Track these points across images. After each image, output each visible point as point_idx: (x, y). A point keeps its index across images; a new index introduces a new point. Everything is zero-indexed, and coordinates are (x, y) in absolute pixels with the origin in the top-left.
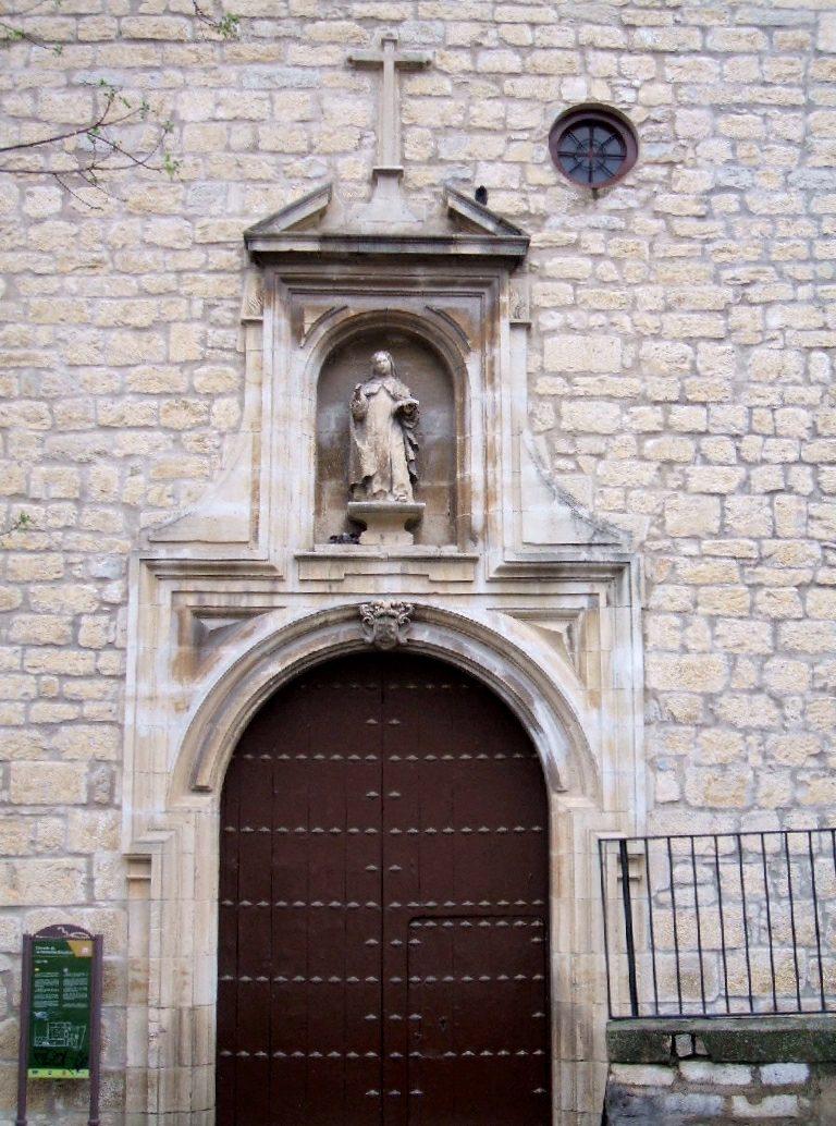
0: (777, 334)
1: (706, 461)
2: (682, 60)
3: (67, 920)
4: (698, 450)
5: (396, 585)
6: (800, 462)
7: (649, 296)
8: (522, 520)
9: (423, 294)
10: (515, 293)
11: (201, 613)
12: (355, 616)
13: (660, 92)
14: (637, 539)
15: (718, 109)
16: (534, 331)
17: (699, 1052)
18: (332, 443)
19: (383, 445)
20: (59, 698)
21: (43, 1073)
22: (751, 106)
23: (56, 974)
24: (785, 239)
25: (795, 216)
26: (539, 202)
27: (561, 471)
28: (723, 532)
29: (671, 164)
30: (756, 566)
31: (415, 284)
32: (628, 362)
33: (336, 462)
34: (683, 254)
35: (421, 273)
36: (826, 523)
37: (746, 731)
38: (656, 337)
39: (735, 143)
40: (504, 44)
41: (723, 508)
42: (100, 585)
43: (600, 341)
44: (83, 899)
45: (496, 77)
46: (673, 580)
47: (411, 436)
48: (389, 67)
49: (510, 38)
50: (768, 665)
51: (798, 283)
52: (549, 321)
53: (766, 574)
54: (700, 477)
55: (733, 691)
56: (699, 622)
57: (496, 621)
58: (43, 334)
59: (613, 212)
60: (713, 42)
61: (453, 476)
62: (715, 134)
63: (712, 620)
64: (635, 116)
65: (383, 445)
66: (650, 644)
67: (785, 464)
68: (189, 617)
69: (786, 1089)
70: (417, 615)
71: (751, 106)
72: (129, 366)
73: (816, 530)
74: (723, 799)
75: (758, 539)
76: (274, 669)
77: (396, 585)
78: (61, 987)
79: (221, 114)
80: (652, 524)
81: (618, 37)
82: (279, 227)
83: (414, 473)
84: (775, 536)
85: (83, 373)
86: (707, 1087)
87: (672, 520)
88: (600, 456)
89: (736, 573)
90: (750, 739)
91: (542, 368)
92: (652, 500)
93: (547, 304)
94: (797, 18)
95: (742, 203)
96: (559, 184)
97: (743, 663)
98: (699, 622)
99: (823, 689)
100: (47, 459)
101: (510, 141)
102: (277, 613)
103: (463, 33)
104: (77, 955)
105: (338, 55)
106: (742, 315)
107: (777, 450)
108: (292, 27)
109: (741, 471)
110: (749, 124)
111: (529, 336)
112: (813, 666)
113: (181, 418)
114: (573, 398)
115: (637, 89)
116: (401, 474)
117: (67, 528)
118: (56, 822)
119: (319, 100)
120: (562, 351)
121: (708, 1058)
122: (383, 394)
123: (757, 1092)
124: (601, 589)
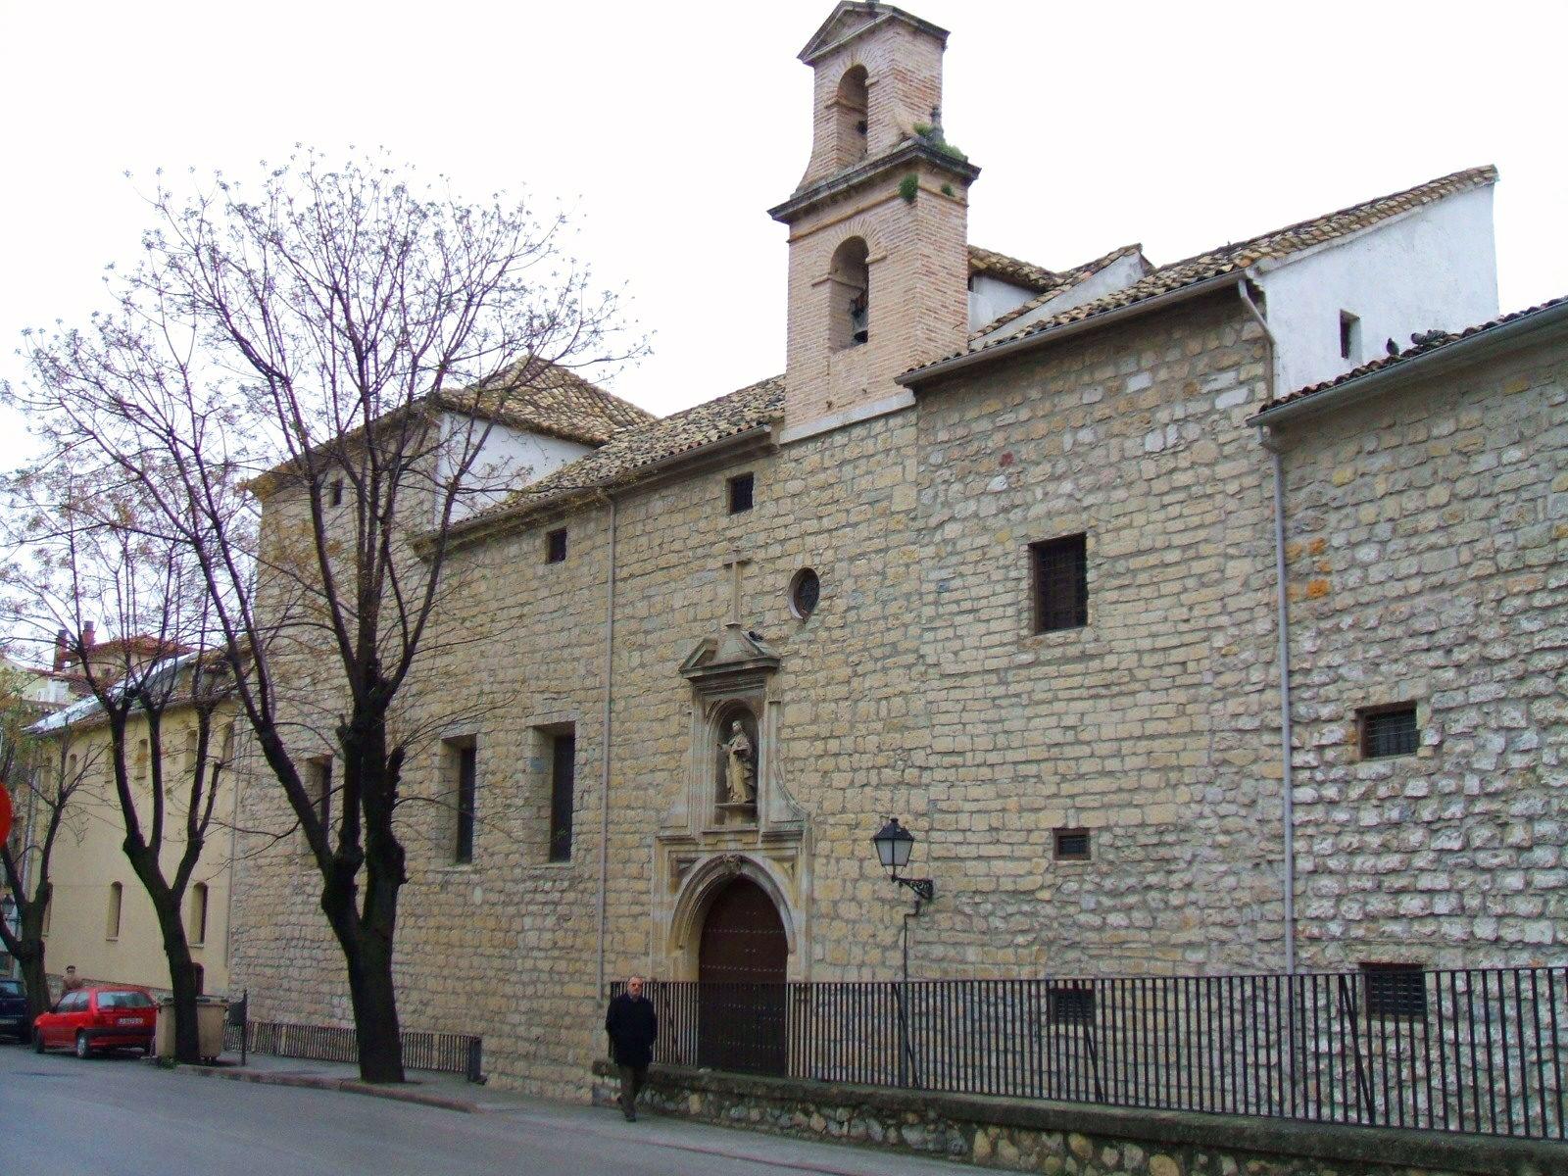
5: (732, 846)
8: (773, 810)
10: (773, 682)
11: (680, 861)
15: (852, 559)
28: (843, 811)
37: (847, 921)
63: (838, 860)
64: (818, 573)
65: (736, 773)
76: (700, 888)
77: (732, 846)
87: (826, 804)
106: (856, 683)
108: (707, 550)
120: (791, 714)
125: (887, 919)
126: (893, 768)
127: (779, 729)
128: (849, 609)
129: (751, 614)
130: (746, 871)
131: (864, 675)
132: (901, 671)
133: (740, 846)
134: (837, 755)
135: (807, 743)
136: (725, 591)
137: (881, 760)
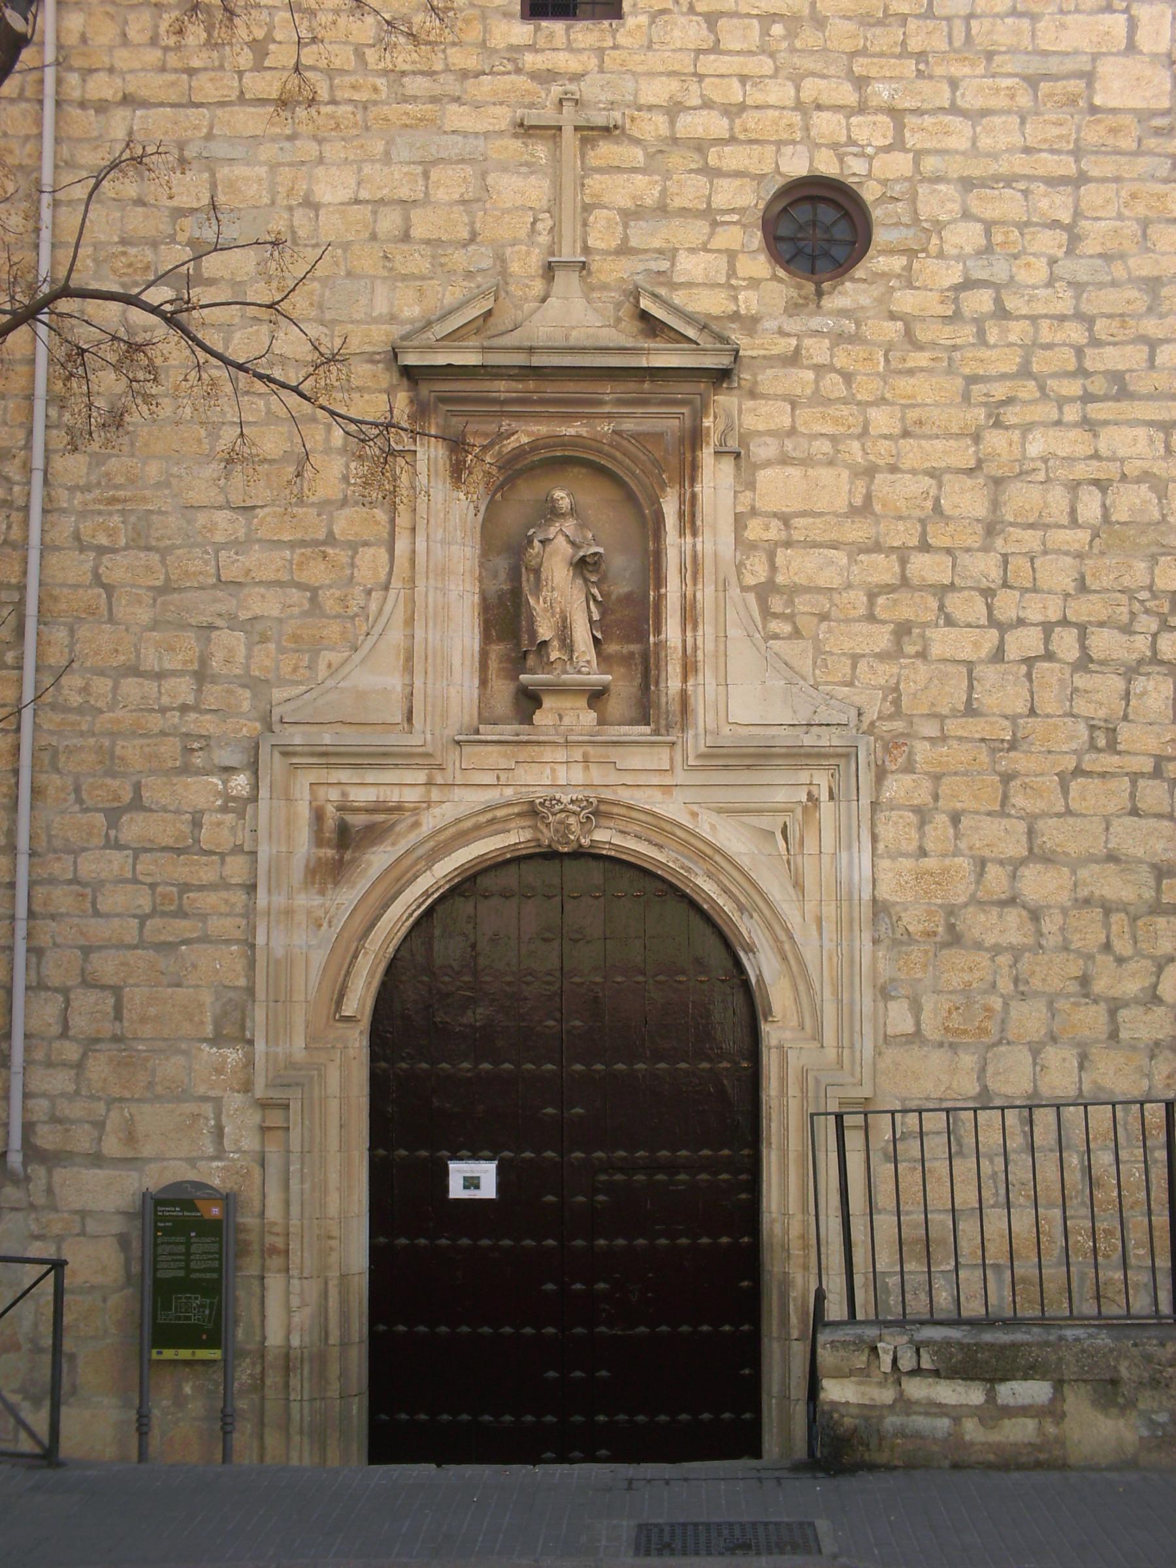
0: (1039, 464)
1: (950, 622)
2: (928, 120)
3: (192, 1176)
4: (941, 607)
5: (577, 775)
6: (1064, 622)
7: (882, 420)
9: (609, 416)
13: (901, 164)
14: (866, 721)
15: (967, 184)
16: (743, 463)
18: (500, 597)
19: (562, 601)
21: (169, 1354)
22: (1009, 181)
23: (182, 1239)
24: (1049, 346)
25: (1062, 318)
26: (748, 302)
27: (776, 637)
29: (911, 253)
30: (1009, 750)
31: (601, 403)
32: (858, 501)
33: (506, 621)
34: (924, 364)
35: (607, 391)
38: (894, 469)
39: (989, 226)
40: (708, 104)
42: (225, 776)
43: (825, 474)
44: (210, 1150)
45: (700, 146)
46: (909, 768)
47: (595, 591)
48: (568, 131)
49: (717, 97)
51: (1062, 402)
52: (762, 450)
53: (1019, 761)
54: (943, 642)
55: (980, 903)
57: (694, 815)
58: (153, 470)
59: (843, 313)
60: (969, 99)
61: (642, 637)
62: (967, 215)
64: (870, 193)
66: (881, 846)
67: (1048, 628)
69: (1024, 1411)
71: (1009, 181)
72: (254, 508)
73: (1082, 707)
74: (965, 1032)
75: (1013, 719)
78: (188, 1253)
79: (364, 195)
80: (884, 699)
81: (847, 94)
82: (430, 336)
83: (599, 636)
85: (202, 518)
86: (936, 1409)
88: (824, 617)
89: (984, 757)
91: (753, 508)
92: (886, 672)
93: (761, 427)
94: (1070, 65)
95: (998, 301)
96: (775, 277)
97: (992, 871)
98: (942, 819)
99: (1087, 902)
101: (715, 224)
102: (436, 811)
103: (656, 91)
104: (206, 1217)
105: (502, 117)
106: (996, 440)
108: (449, 84)
109: (994, 633)
110: (1006, 205)
111: (738, 467)
113: (316, 573)
114: (788, 544)
115: (871, 158)
116: (582, 635)
117: (184, 709)
118: (180, 1060)
119: (484, 175)
120: (777, 487)
121: (936, 1373)
122: (561, 539)
123: (993, 1413)
124: (822, 780)
125: (1122, 946)
126: (1127, 629)
127: (740, 522)
128: (969, 284)
129: (624, 250)
130: (604, 836)
131: (1027, 428)
132: (1141, 432)
133: (597, 775)
134: (943, 591)
135: (841, 557)
136: (521, 189)
137: (1081, 610)
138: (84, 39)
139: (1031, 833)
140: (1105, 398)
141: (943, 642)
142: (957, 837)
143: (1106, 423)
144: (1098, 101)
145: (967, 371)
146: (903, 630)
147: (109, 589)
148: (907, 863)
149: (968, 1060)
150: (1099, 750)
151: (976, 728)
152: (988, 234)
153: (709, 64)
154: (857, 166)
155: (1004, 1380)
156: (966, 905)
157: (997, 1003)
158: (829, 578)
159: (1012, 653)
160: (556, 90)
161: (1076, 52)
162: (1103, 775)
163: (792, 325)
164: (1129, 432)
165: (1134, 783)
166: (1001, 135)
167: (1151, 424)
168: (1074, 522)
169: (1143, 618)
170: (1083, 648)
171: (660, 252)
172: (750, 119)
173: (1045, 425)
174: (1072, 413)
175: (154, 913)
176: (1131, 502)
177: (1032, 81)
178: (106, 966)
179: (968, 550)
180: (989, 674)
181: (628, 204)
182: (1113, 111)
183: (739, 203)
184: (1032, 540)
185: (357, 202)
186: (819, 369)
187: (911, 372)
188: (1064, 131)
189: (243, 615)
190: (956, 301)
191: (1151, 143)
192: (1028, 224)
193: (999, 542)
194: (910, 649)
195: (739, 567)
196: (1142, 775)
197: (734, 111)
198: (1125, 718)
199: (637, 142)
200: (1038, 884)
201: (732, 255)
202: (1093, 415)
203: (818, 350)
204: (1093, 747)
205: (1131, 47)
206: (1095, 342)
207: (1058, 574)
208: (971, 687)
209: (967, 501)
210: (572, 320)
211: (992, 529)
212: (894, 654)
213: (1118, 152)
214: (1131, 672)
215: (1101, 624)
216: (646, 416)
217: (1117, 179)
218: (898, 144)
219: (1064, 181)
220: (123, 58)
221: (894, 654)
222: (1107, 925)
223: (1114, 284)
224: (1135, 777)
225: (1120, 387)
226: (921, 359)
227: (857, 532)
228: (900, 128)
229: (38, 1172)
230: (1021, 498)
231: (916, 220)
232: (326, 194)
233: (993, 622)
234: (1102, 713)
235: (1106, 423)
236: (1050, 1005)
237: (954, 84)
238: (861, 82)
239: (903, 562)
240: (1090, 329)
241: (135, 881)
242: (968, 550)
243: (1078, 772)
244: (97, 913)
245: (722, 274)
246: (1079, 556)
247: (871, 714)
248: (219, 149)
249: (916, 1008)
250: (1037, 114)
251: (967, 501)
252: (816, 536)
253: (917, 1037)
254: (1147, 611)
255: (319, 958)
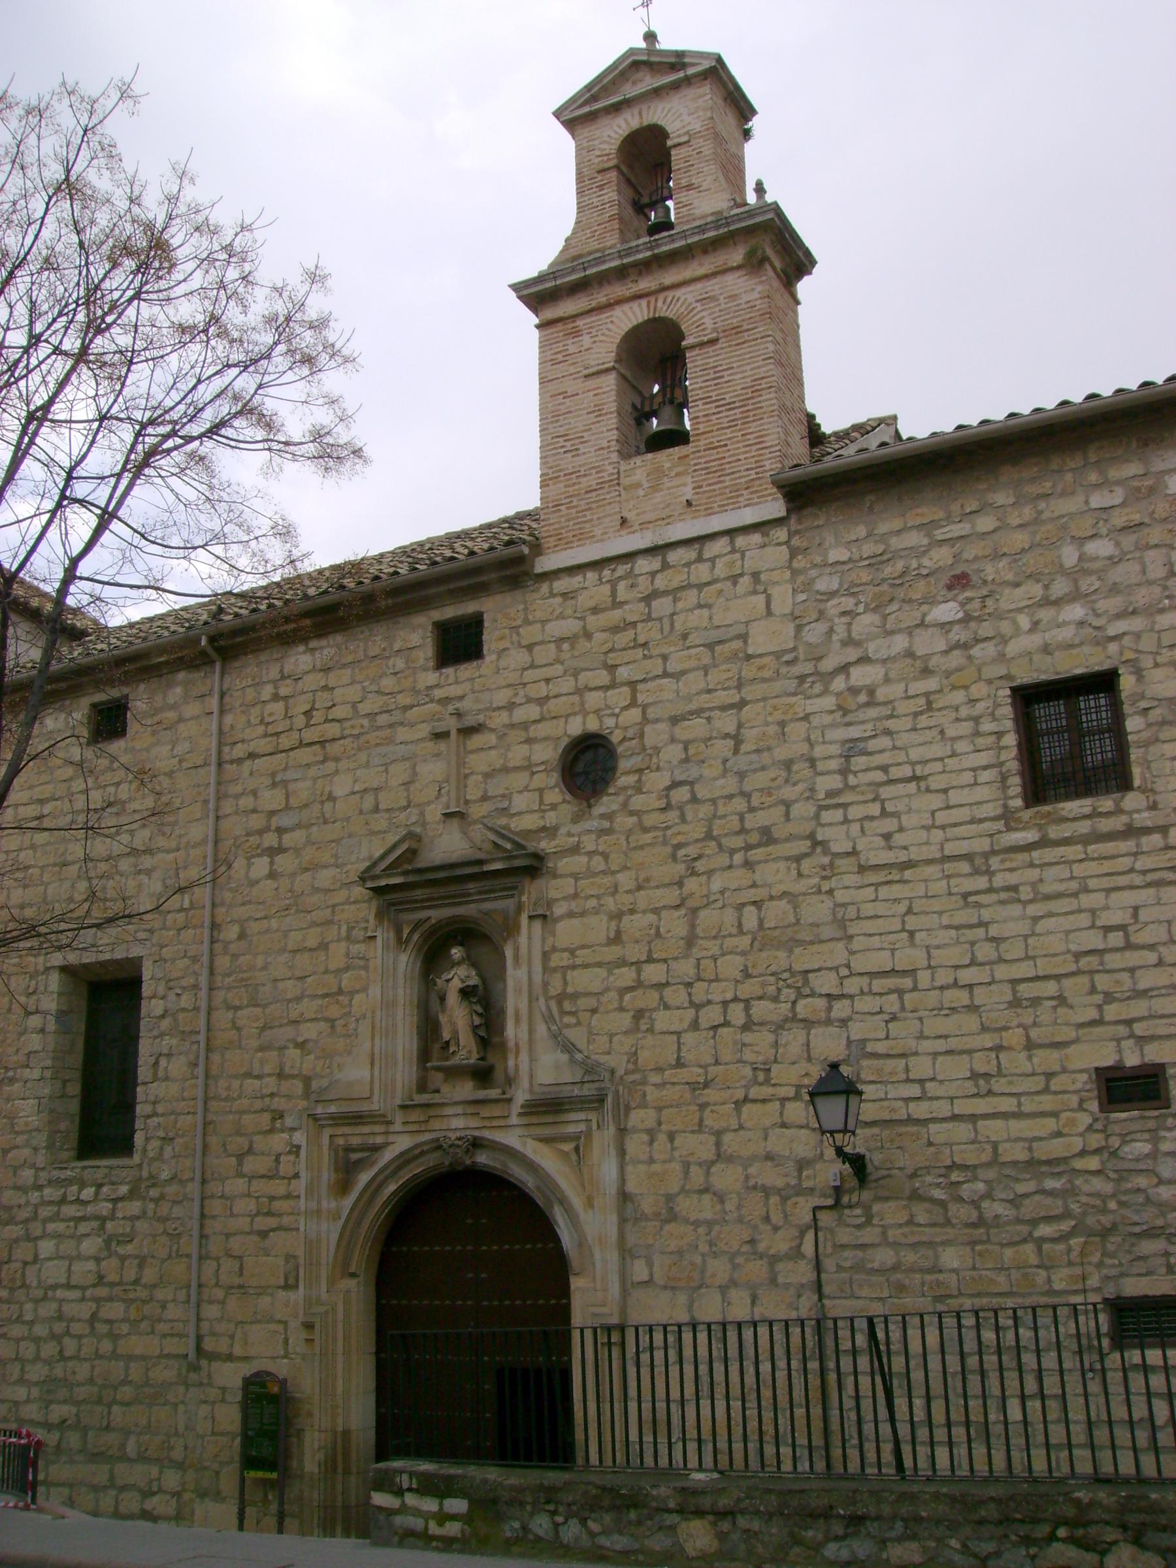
0: (718, 896)
1: (667, 1007)
2: (650, 685)
4: (661, 998)
6: (735, 999)
7: (625, 880)
8: (536, 1065)
10: (531, 891)
11: (349, 1149)
12: (437, 1146)
13: (634, 714)
15: (675, 720)
17: (414, 1486)
20: (269, 1214)
22: (698, 712)
24: (724, 816)
25: (731, 797)
26: (551, 818)
27: (568, 1026)
28: (679, 1064)
29: (640, 771)
31: (469, 895)
32: (612, 935)
35: (472, 886)
36: (756, 1048)
37: (697, 1224)
38: (632, 911)
39: (686, 746)
40: (529, 700)
41: (679, 1044)
43: (592, 920)
45: (525, 725)
46: (643, 1105)
48: (454, 733)
49: (533, 695)
50: (713, 1169)
51: (732, 852)
53: (710, 1095)
54: (663, 1020)
55: (688, 1192)
56: (662, 1138)
58: (260, 961)
59: (603, 816)
60: (672, 667)
62: (673, 740)
63: (671, 1137)
64: (615, 738)
65: (457, 1018)
66: (627, 1157)
67: (725, 1004)
68: (341, 1153)
70: (477, 1144)
71: (698, 712)
73: (748, 1056)
75: (705, 1067)
76: (392, 1187)
77: (458, 1123)
79: (357, 788)
81: (603, 677)
82: (378, 870)
84: (717, 1063)
85: (281, 985)
87: (644, 1055)
88: (594, 1011)
89: (688, 1096)
90: (700, 1230)
92: (628, 1042)
93: (559, 896)
94: (733, 631)
95: (693, 793)
96: (564, 801)
97: (694, 1169)
98: (662, 1138)
99: (755, 1187)
100: (262, 1049)
101: (533, 773)
102: (390, 1148)
103: (501, 697)
105: (424, 730)
106: (692, 884)
107: (721, 991)
108: (397, 716)
109: (693, 1011)
110: (695, 728)
112: (745, 1169)
113: (334, 1011)
115: (617, 716)
117: (272, 1095)
118: (268, 1299)
119: (415, 765)
120: (567, 932)
124: (593, 1116)
125: (776, 1218)
126: (775, 999)
127: (546, 956)
128: (675, 785)
129: (485, 798)
130: (482, 1158)
131: (710, 873)
132: (782, 865)
133: (473, 1123)
134: (660, 986)
135: (602, 972)
136: (433, 770)
137: (748, 989)
138: (232, 727)
139: (718, 1144)
140: (759, 845)
141: (663, 1020)
142: (673, 1149)
143: (759, 862)
144: (750, 652)
145: (675, 842)
146: (639, 1014)
147: (239, 1029)
148: (642, 1168)
149: (682, 1298)
150: (761, 1084)
151: (684, 1074)
152: (686, 749)
153: (529, 675)
154: (610, 722)
155: (449, 1496)
156: (679, 1194)
157: (698, 1260)
158: (596, 986)
159: (704, 1023)
160: (451, 708)
161: (736, 622)
162: (764, 1101)
163: (576, 829)
164: (773, 866)
165: (783, 1106)
166: (695, 681)
167: (787, 859)
168: (741, 932)
169: (785, 991)
170: (748, 1016)
171: (503, 796)
172: (552, 704)
173: (723, 869)
174: (738, 858)
175: (258, 1213)
176: (777, 911)
177: (710, 646)
178: (235, 1244)
179: (676, 959)
180: (689, 1038)
181: (488, 770)
182: (761, 656)
183: (545, 758)
184: (714, 948)
185: (354, 793)
186: (590, 854)
187: (642, 847)
188: (730, 674)
189: (300, 1039)
190: (667, 796)
191: (784, 670)
192: (710, 739)
193: (694, 950)
194: (644, 1027)
195: (546, 984)
196: (788, 1099)
197: (542, 701)
198: (776, 1061)
199: (492, 730)
200: (726, 1178)
201: (541, 791)
202: (751, 859)
203: (589, 843)
204: (755, 1082)
205: (769, 613)
206: (752, 810)
207: (731, 966)
208: (679, 1049)
209: (675, 925)
210: (448, 845)
211: (690, 941)
212: (635, 1029)
213: (764, 680)
214: (779, 1027)
215: (760, 998)
216: (496, 899)
217: (764, 699)
218: (633, 703)
219: (731, 706)
220: (248, 734)
221: (635, 1029)
222: (766, 1204)
223: (763, 768)
224: (784, 1100)
225: (767, 836)
226: (648, 838)
227: (613, 953)
228: (634, 692)
229: (204, 1363)
230: (707, 918)
231: (644, 749)
232: (339, 792)
233: (692, 1004)
234: (761, 1058)
235: (759, 862)
236: (731, 1260)
237: (665, 658)
238: (612, 668)
239: (639, 972)
240: (749, 802)
241: (249, 1195)
242: (676, 959)
243: (746, 1100)
244: (232, 1215)
245: (532, 803)
246: (743, 953)
247: (620, 1072)
248: (291, 774)
249: (650, 1264)
250: (715, 666)
251: (675, 925)
252: (591, 960)
253: (649, 1282)
254: (789, 987)
255: (334, 1237)
